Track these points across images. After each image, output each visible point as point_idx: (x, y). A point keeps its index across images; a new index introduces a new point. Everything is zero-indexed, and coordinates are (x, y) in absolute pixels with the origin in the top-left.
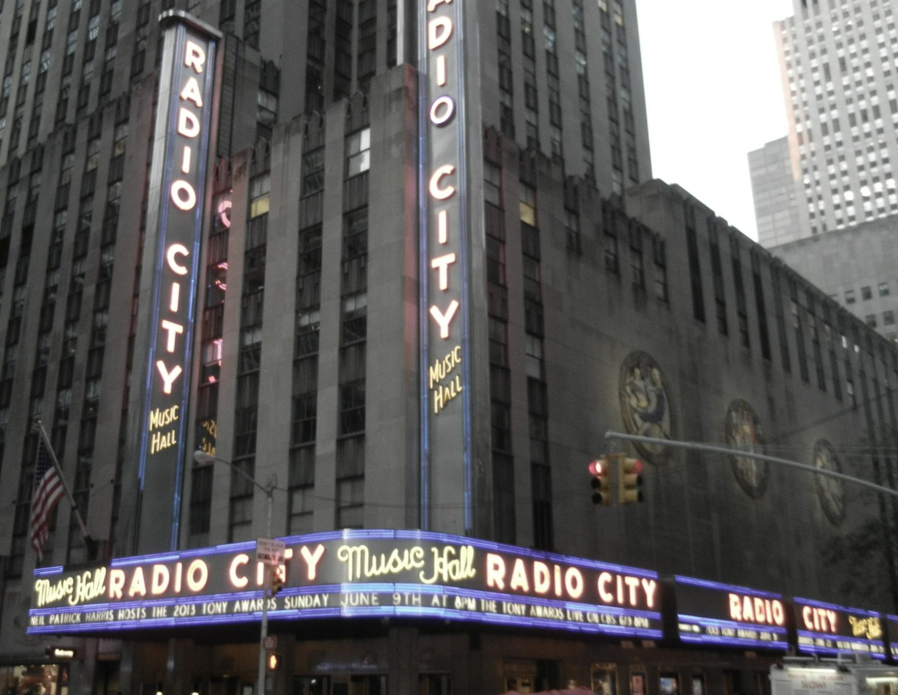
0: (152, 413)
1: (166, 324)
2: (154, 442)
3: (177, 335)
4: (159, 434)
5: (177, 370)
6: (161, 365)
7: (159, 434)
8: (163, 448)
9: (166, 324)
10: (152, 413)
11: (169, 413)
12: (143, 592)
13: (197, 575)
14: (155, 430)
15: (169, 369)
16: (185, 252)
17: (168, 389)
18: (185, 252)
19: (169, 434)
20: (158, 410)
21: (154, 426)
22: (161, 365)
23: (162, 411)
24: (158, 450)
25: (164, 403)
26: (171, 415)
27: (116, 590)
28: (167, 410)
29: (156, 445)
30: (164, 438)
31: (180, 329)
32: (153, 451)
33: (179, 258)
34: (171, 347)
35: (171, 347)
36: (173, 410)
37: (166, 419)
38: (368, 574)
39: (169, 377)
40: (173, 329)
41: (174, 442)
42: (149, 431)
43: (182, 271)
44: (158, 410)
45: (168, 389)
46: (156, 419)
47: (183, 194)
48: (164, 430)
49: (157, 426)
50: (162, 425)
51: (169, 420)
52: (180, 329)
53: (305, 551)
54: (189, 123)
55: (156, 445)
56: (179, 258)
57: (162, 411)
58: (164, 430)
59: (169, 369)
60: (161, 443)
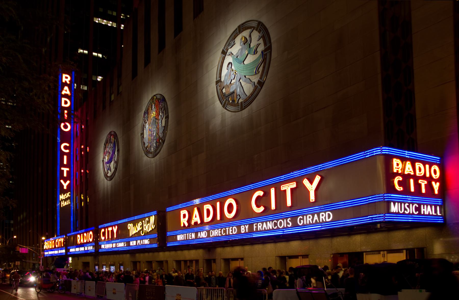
0: (60, 195)
1: (62, 169)
2: (62, 203)
3: (67, 171)
4: (63, 201)
5: (68, 182)
6: (62, 181)
7: (63, 201)
8: (66, 205)
9: (62, 169)
10: (60, 195)
11: (67, 195)
14: (62, 200)
15: (65, 182)
16: (68, 145)
17: (65, 188)
18: (68, 145)
19: (67, 201)
20: (62, 194)
21: (61, 199)
22: (62, 181)
23: (64, 195)
24: (64, 206)
25: (64, 192)
26: (68, 195)
28: (66, 194)
29: (63, 204)
30: (65, 202)
31: (68, 169)
32: (62, 206)
34: (65, 175)
35: (65, 175)
36: (68, 194)
37: (66, 197)
39: (65, 185)
40: (65, 170)
41: (69, 203)
42: (60, 201)
43: (67, 151)
44: (62, 194)
45: (65, 188)
46: (62, 197)
48: (66, 200)
49: (62, 199)
50: (64, 199)
51: (67, 197)
52: (68, 169)
55: (63, 204)
57: (64, 195)
58: (66, 200)
59: (65, 182)
60: (64, 204)
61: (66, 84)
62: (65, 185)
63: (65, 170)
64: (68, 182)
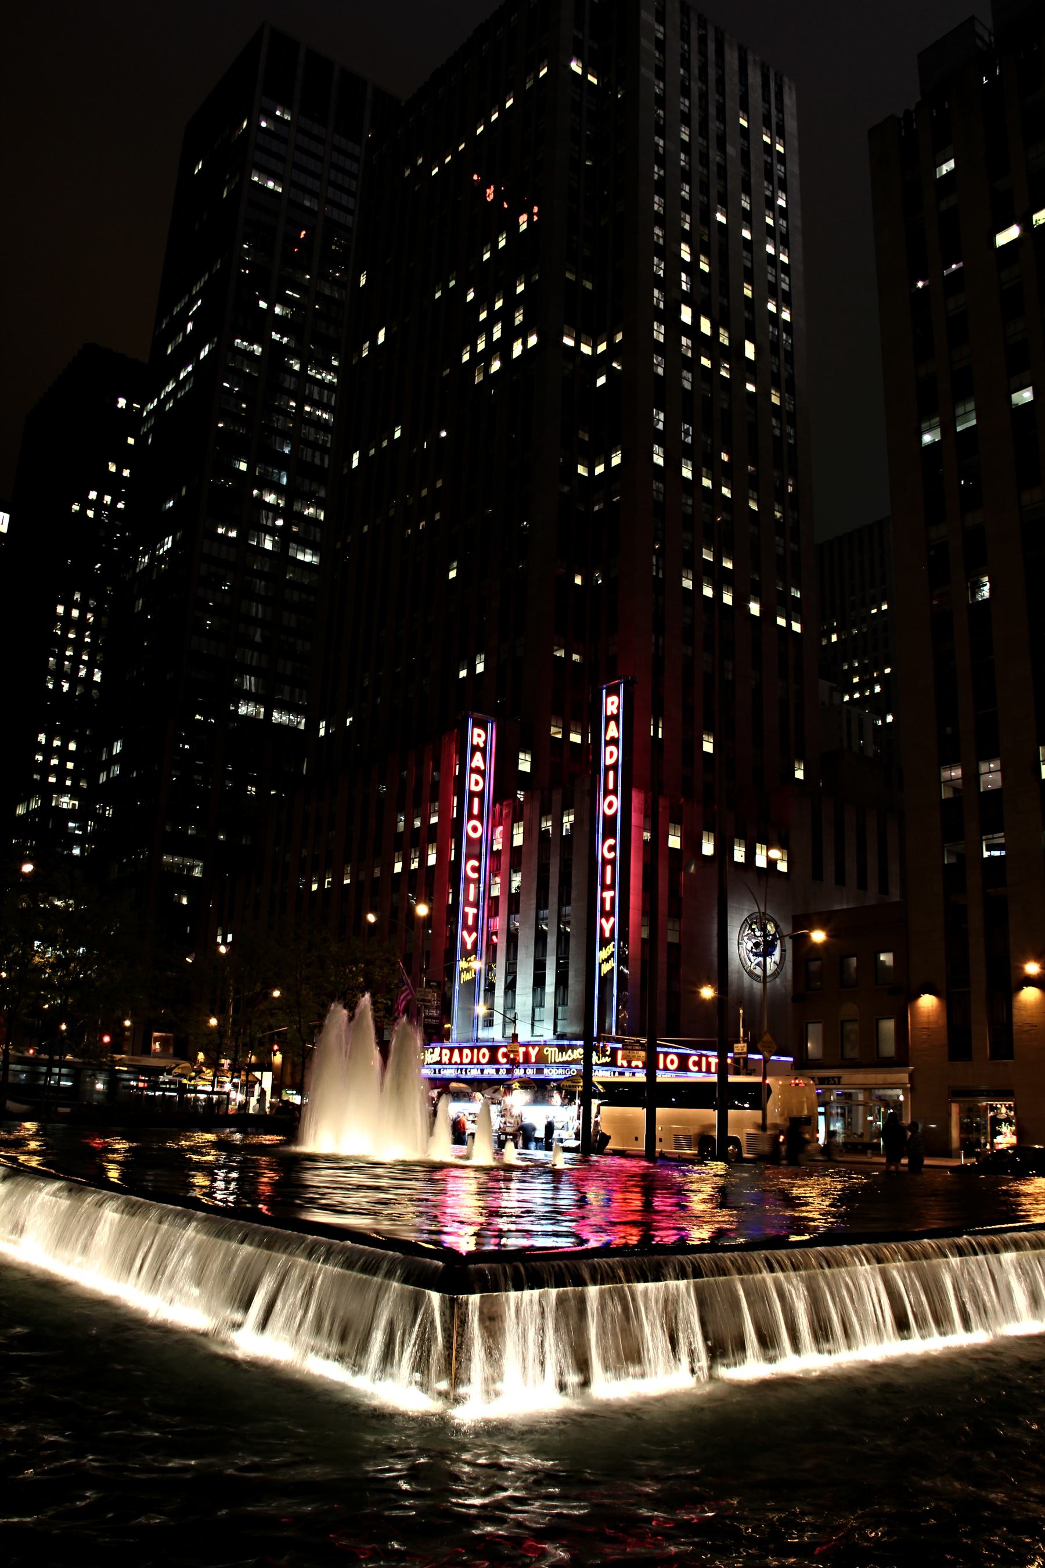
1: (467, 909)
5: (474, 935)
9: (467, 909)
12: (459, 1062)
13: (484, 1055)
14: (463, 970)
15: (470, 935)
16: (476, 863)
17: (469, 947)
18: (476, 863)
22: (465, 933)
27: (445, 1059)
31: (475, 911)
33: (475, 869)
34: (470, 922)
35: (470, 922)
38: (557, 1061)
39: (469, 940)
40: (471, 911)
43: (475, 876)
45: (469, 947)
47: (475, 829)
52: (475, 911)
53: (530, 1049)
54: (477, 783)
56: (475, 869)
59: (470, 935)
61: (475, 748)
62: (469, 940)
63: (471, 911)
64: (474, 935)
